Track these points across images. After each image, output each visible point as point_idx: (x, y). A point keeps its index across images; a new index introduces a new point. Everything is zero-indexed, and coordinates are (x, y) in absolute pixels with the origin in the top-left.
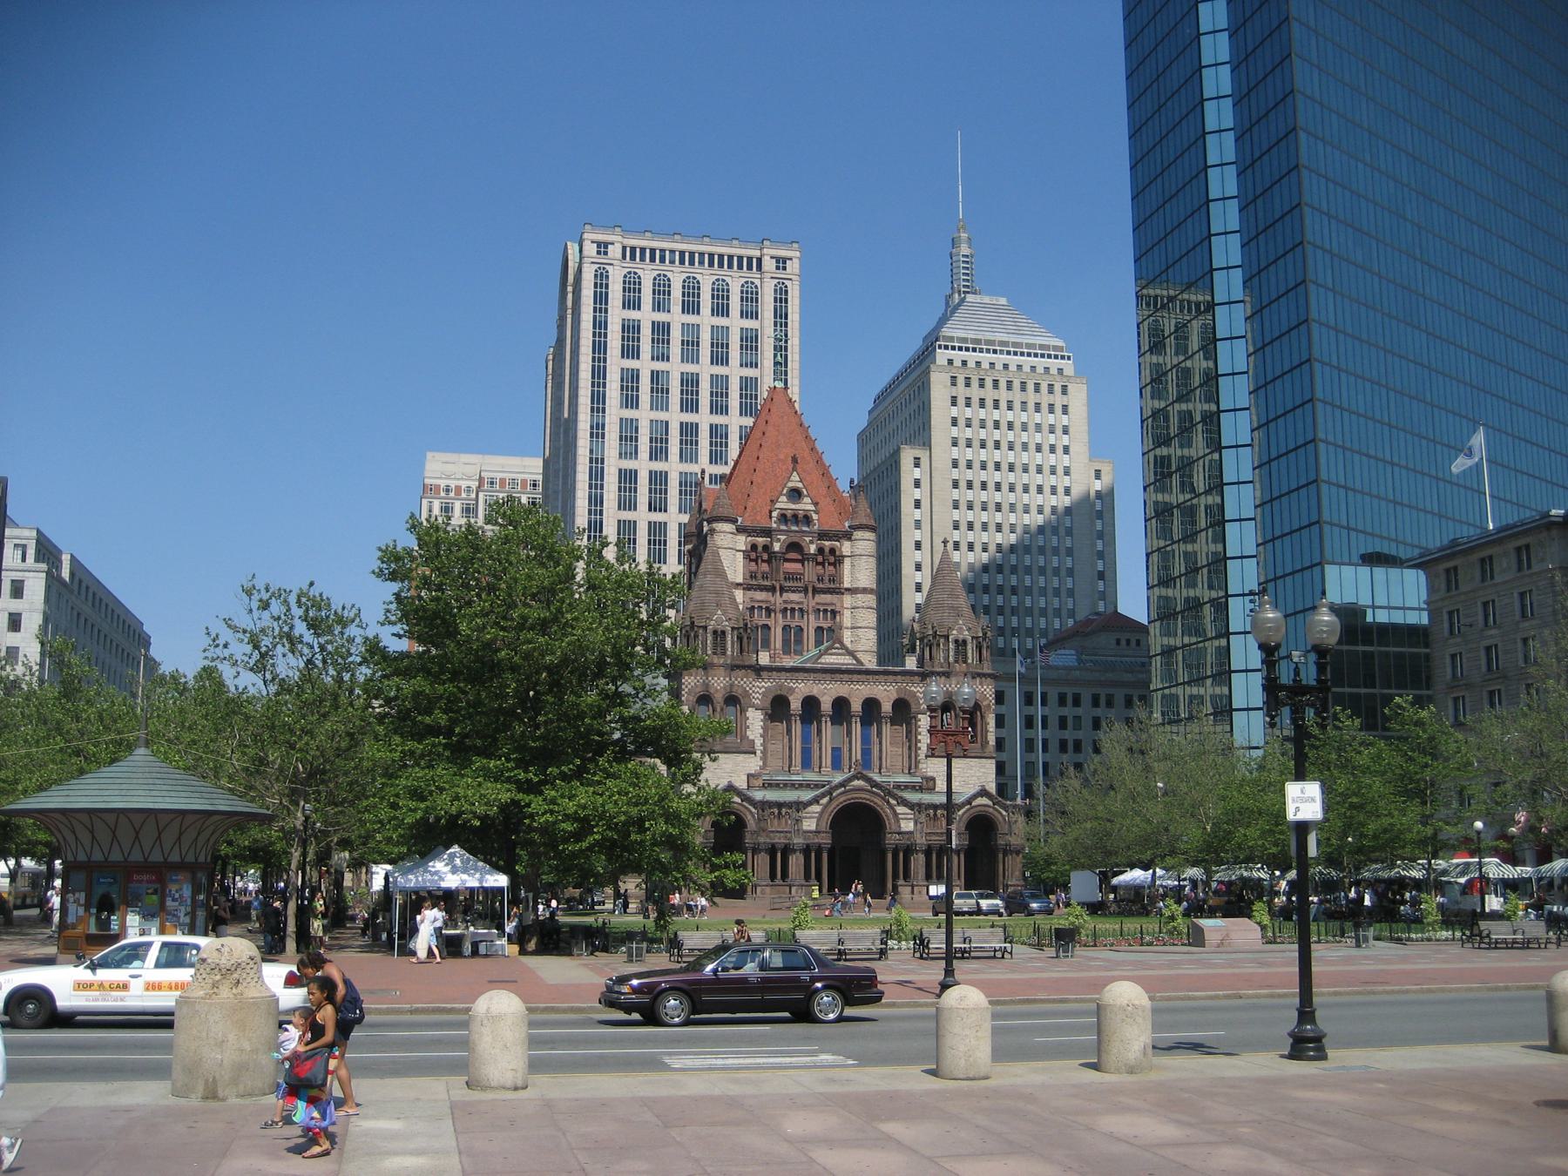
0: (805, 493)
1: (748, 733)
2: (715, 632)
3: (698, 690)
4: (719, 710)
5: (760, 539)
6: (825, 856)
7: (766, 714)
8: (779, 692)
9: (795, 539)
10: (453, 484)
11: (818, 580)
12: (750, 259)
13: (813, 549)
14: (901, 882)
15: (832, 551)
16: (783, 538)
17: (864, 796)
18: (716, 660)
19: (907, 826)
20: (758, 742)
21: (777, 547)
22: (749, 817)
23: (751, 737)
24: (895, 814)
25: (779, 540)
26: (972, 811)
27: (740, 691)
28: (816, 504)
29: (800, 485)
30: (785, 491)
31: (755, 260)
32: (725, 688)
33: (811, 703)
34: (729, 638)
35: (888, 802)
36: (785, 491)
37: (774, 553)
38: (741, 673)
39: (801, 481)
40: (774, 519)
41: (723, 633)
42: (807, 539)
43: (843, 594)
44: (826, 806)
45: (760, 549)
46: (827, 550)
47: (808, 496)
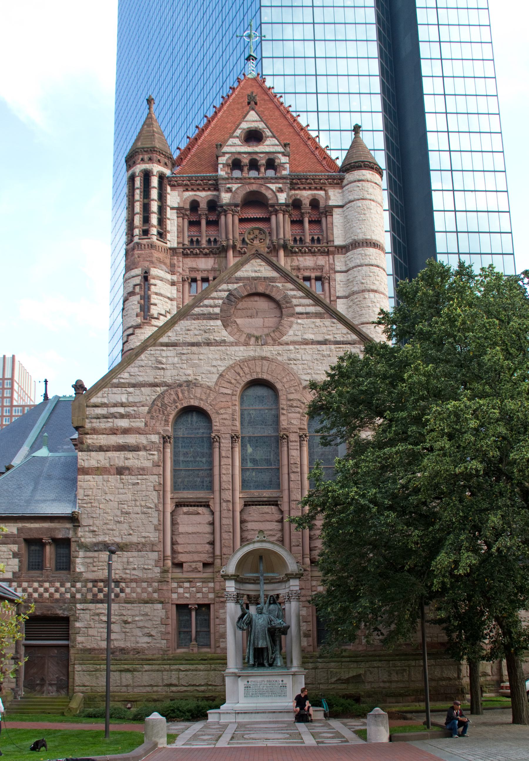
0: (269, 133)
5: (203, 194)
9: (254, 187)
11: (295, 240)
13: (282, 198)
15: (315, 203)
16: (234, 187)
21: (226, 198)
25: (229, 190)
28: (285, 145)
29: (261, 125)
30: (238, 132)
36: (238, 132)
37: (222, 206)
39: (262, 121)
40: (220, 166)
42: (273, 187)
43: (333, 254)
45: (203, 205)
46: (306, 202)
47: (274, 137)
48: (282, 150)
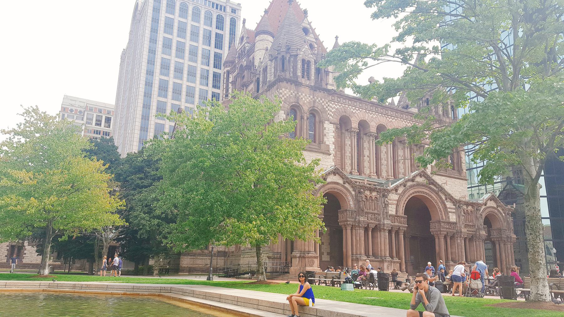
0: (311, 31)
1: (325, 139)
2: (303, 61)
3: (292, 101)
4: (305, 118)
6: (402, 236)
7: (337, 128)
8: (344, 114)
10: (74, 108)
12: (221, 6)
14: (451, 263)
17: (425, 191)
18: (303, 81)
19: (453, 218)
20: (332, 147)
22: (350, 198)
23: (327, 143)
24: (445, 207)
26: (487, 211)
27: (320, 107)
31: (223, 7)
32: (309, 103)
33: (363, 124)
34: (313, 67)
35: (441, 198)
38: (321, 94)
41: (309, 62)
44: (401, 195)
48: (315, 41)
